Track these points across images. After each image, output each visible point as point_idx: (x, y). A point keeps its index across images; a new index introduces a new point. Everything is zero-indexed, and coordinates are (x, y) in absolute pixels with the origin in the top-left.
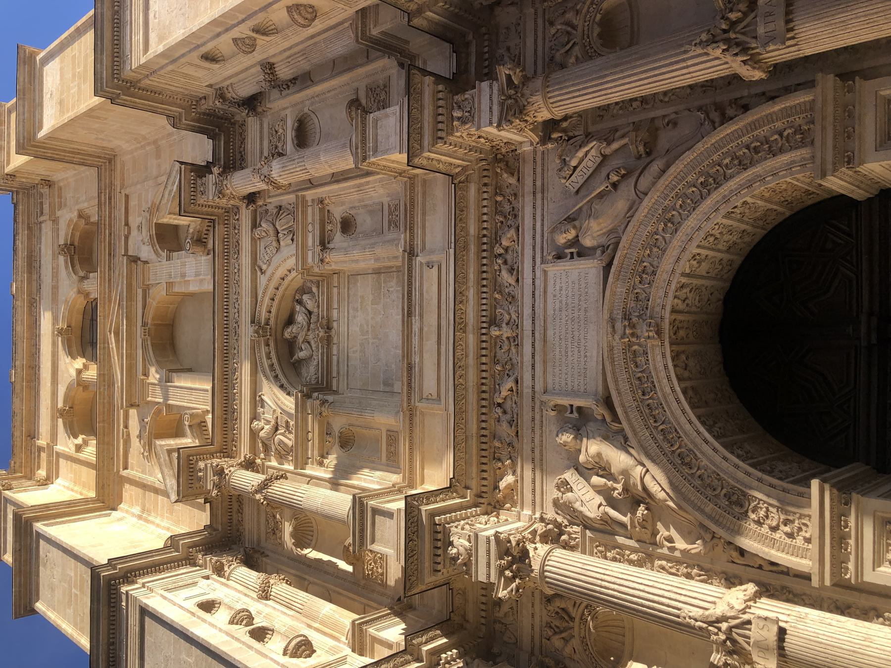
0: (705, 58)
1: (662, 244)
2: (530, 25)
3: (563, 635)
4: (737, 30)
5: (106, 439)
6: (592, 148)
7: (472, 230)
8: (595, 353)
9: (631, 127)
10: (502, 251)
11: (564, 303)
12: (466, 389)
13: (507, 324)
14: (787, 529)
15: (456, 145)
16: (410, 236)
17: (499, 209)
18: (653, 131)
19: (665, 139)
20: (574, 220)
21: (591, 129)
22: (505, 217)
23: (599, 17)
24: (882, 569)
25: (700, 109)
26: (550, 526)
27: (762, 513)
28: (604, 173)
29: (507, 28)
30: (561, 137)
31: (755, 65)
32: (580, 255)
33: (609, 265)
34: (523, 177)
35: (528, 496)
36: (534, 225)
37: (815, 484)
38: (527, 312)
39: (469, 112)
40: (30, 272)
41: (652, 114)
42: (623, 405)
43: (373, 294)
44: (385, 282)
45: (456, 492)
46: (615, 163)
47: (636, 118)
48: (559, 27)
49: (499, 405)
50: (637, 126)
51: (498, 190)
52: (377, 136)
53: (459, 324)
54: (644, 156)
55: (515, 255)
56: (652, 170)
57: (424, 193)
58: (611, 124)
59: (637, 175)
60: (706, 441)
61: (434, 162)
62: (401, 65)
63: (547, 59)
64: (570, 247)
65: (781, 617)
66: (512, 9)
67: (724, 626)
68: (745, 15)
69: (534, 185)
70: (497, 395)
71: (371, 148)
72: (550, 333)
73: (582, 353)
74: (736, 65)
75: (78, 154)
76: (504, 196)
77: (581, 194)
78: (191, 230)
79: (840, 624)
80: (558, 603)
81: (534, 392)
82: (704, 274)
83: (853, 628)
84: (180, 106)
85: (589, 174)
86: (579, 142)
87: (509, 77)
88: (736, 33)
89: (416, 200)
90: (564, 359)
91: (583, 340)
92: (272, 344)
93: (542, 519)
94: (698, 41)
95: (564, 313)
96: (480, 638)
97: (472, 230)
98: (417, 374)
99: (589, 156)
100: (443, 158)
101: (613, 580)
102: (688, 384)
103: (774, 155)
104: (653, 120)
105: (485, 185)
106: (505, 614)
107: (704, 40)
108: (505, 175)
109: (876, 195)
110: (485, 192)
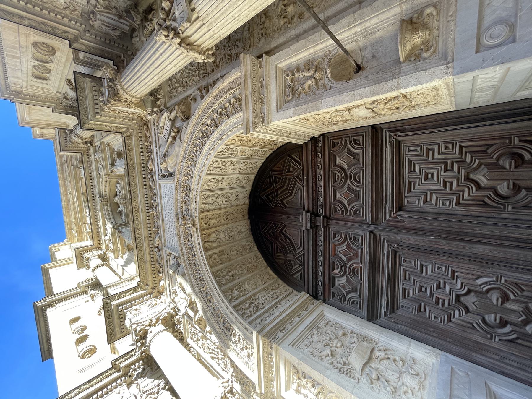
5: (81, 235)
12: (142, 239)
31: (188, 47)
40: (62, 170)
45: (141, 288)
53: (135, 208)
75: (51, 125)
78: (79, 157)
84: (53, 103)
92: (108, 205)
109: (309, 141)
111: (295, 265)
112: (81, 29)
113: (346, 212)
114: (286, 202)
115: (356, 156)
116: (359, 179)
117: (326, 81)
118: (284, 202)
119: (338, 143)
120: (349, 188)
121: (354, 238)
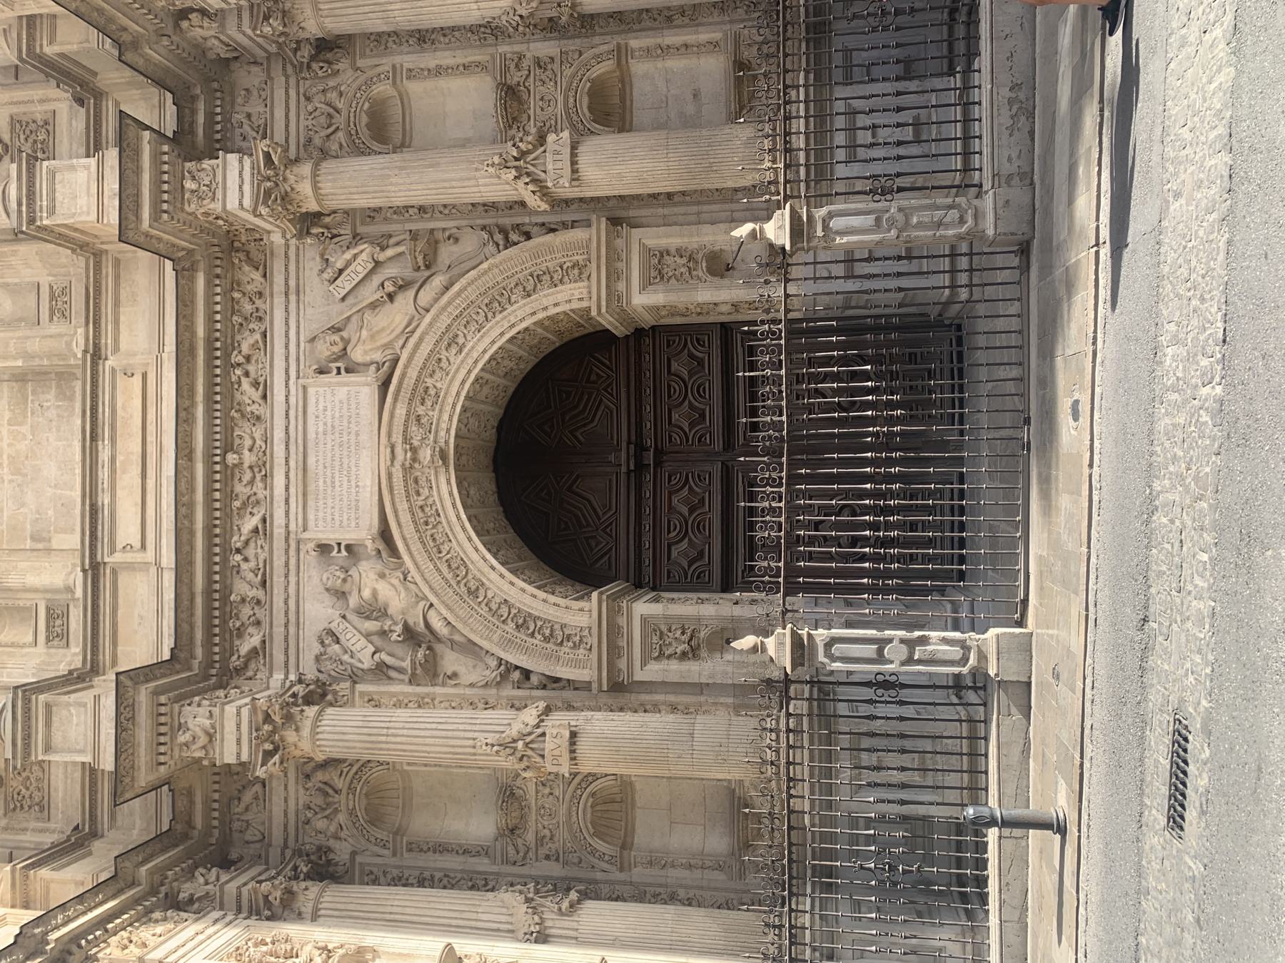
0: (495, 181)
1: (444, 364)
2: (279, 94)
3: (328, 812)
4: (528, 160)
6: (362, 251)
7: (201, 331)
8: (369, 483)
9: (407, 236)
10: (240, 359)
11: (329, 425)
13: (250, 450)
14: (570, 644)
15: (184, 223)
16: (94, 331)
17: (236, 307)
18: (434, 245)
19: (447, 253)
20: (339, 330)
21: (360, 229)
22: (246, 319)
23: (367, 105)
24: (648, 667)
25: (484, 228)
26: (312, 687)
27: (547, 632)
28: (376, 280)
29: (247, 90)
30: (323, 233)
32: (348, 371)
33: (385, 385)
34: (272, 273)
35: (279, 657)
36: (287, 333)
37: (595, 595)
38: (279, 435)
39: (207, 186)
41: (431, 225)
42: (404, 539)
43: (10, 410)
44: (34, 392)
46: (391, 271)
47: (413, 226)
48: (318, 105)
49: (238, 551)
50: (414, 236)
51: (235, 285)
52: (54, 191)
53: (183, 449)
54: (422, 268)
55: (260, 366)
56: (434, 284)
57: (117, 278)
58: (385, 228)
59: (416, 288)
60: (493, 568)
61: (153, 241)
62: (80, 101)
63: (302, 140)
64: (335, 360)
65: (573, 723)
66: (255, 69)
67: (520, 744)
68: (535, 148)
69: (287, 284)
70: (235, 538)
71: (45, 209)
72: (311, 460)
73: (353, 483)
74: (525, 192)
76: (244, 294)
77: (350, 300)
79: (621, 718)
80: (320, 776)
81: (288, 533)
82: (484, 399)
83: (632, 719)
85: (357, 280)
86: (345, 243)
87: (267, 156)
88: (526, 162)
89: (104, 283)
90: (329, 492)
91: (354, 469)
93: (300, 681)
94: (490, 162)
95: (329, 438)
96: (212, 845)
97: (201, 331)
98: (106, 519)
99: (359, 260)
100: (166, 237)
101: (401, 725)
102: (473, 511)
103: (556, 286)
104: (432, 231)
105: (218, 276)
106: (247, 809)
107: (496, 162)
108: (246, 268)
110: (217, 285)
111: (598, 544)
112: (151, 28)
113: (687, 441)
114: (581, 434)
115: (700, 363)
116: (705, 393)
117: (701, 274)
118: (578, 434)
119: (674, 342)
120: (691, 406)
121: (699, 476)
